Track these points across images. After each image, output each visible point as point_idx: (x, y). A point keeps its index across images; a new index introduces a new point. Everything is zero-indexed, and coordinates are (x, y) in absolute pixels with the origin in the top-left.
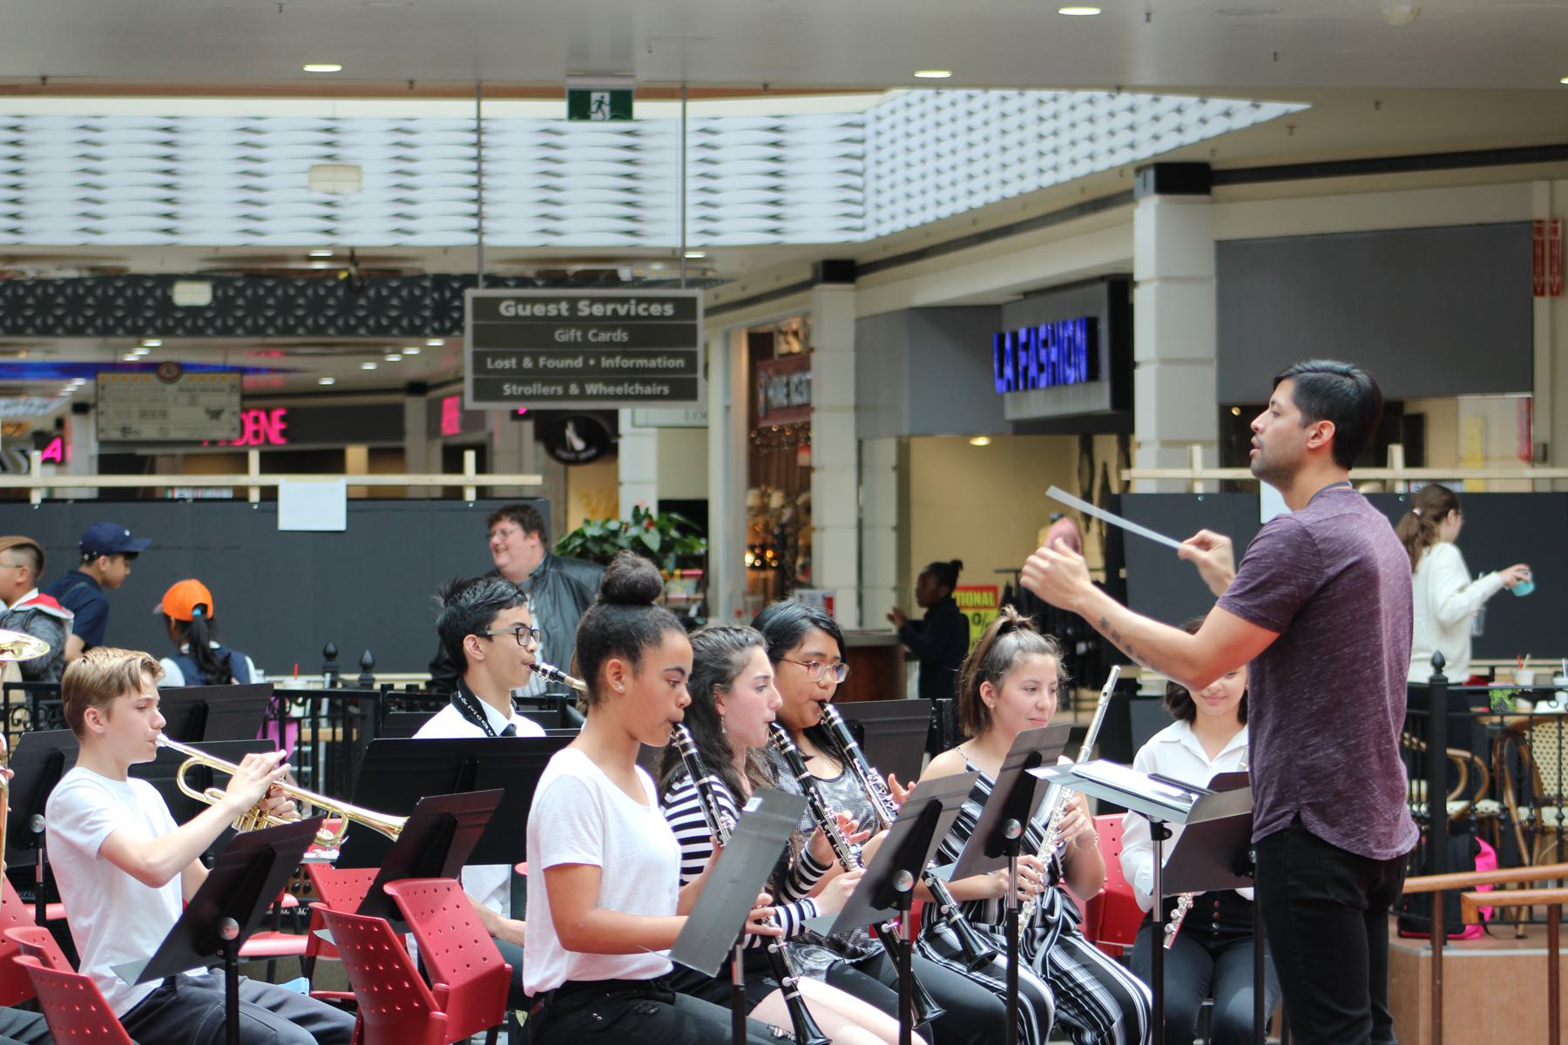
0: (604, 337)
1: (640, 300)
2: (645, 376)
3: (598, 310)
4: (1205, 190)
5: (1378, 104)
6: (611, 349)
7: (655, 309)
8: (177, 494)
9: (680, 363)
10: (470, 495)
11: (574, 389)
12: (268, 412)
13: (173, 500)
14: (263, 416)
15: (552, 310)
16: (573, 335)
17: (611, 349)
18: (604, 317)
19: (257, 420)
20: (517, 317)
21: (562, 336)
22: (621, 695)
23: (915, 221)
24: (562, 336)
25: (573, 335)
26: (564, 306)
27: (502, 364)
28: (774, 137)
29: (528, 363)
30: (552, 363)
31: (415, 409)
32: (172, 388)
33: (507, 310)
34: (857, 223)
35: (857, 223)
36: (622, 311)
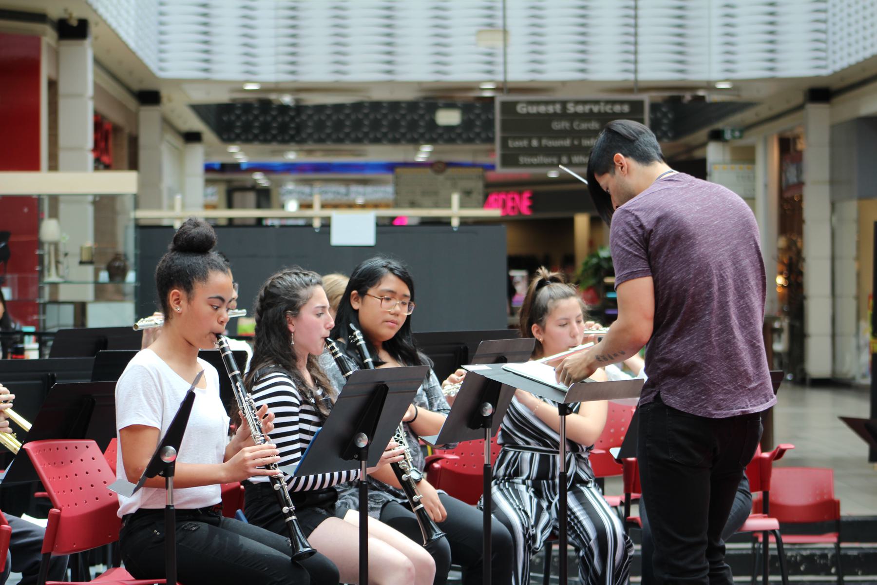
0: (584, 126)
1: (607, 102)
3: (580, 109)
8: (269, 222)
11: (565, 159)
13: (267, 226)
14: (517, 197)
15: (551, 109)
20: (528, 114)
21: (557, 125)
22: (180, 314)
23: (853, 60)
24: (557, 125)
29: (535, 143)
32: (441, 178)
33: (521, 109)
34: (822, 63)
35: (822, 63)
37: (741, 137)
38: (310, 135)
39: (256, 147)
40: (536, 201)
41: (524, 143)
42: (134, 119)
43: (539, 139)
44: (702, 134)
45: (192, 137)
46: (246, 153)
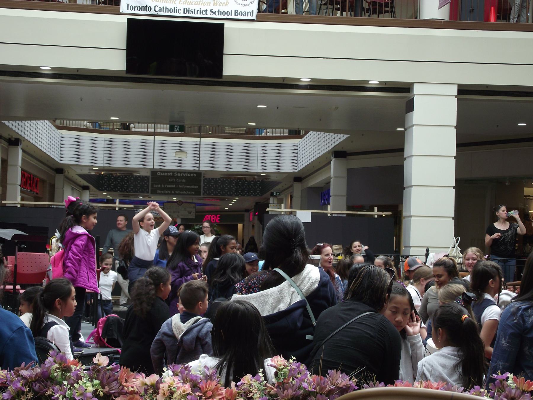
2: (189, 190)
3: (179, 175)
4: (345, 157)
5: (363, 135)
6: (182, 183)
7: (192, 175)
9: (197, 187)
10: (117, 209)
12: (216, 215)
15: (169, 174)
16: (173, 180)
17: (182, 183)
18: (180, 177)
19: (214, 217)
20: (161, 176)
24: (170, 180)
25: (173, 180)
26: (171, 174)
27: (156, 186)
28: (279, 148)
29: (163, 186)
30: (168, 186)
31: (246, 214)
32: (180, 207)
34: (296, 168)
35: (296, 168)
36: (184, 175)
44: (269, 193)
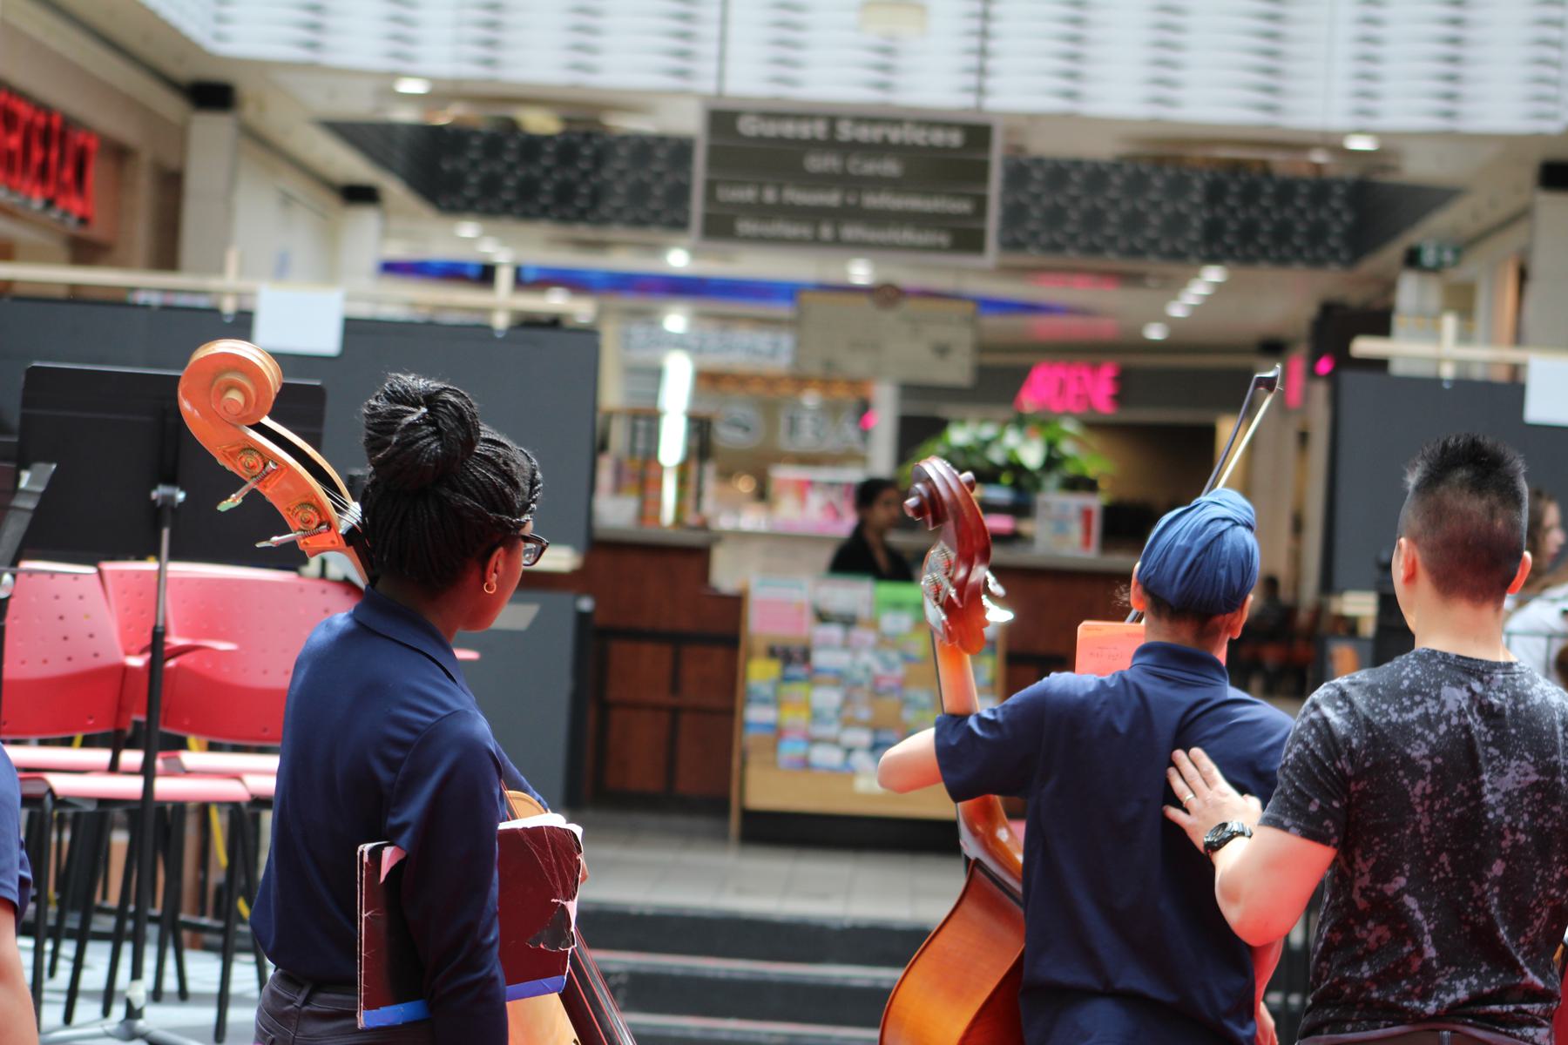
0: (870, 167)
3: (865, 133)
6: (878, 183)
7: (938, 137)
8: (141, 298)
9: (963, 207)
13: (135, 306)
15: (805, 130)
17: (878, 183)
20: (760, 138)
24: (817, 163)
33: (748, 127)
34: (1549, 108)
35: (1549, 108)
37: (1456, 263)
38: (619, 211)
39: (540, 231)
40: (1127, 386)
41: (747, 194)
42: (181, 136)
43: (780, 187)
44: (1394, 252)
45: (359, 195)
46: (505, 241)
